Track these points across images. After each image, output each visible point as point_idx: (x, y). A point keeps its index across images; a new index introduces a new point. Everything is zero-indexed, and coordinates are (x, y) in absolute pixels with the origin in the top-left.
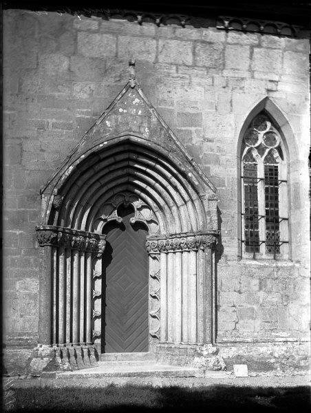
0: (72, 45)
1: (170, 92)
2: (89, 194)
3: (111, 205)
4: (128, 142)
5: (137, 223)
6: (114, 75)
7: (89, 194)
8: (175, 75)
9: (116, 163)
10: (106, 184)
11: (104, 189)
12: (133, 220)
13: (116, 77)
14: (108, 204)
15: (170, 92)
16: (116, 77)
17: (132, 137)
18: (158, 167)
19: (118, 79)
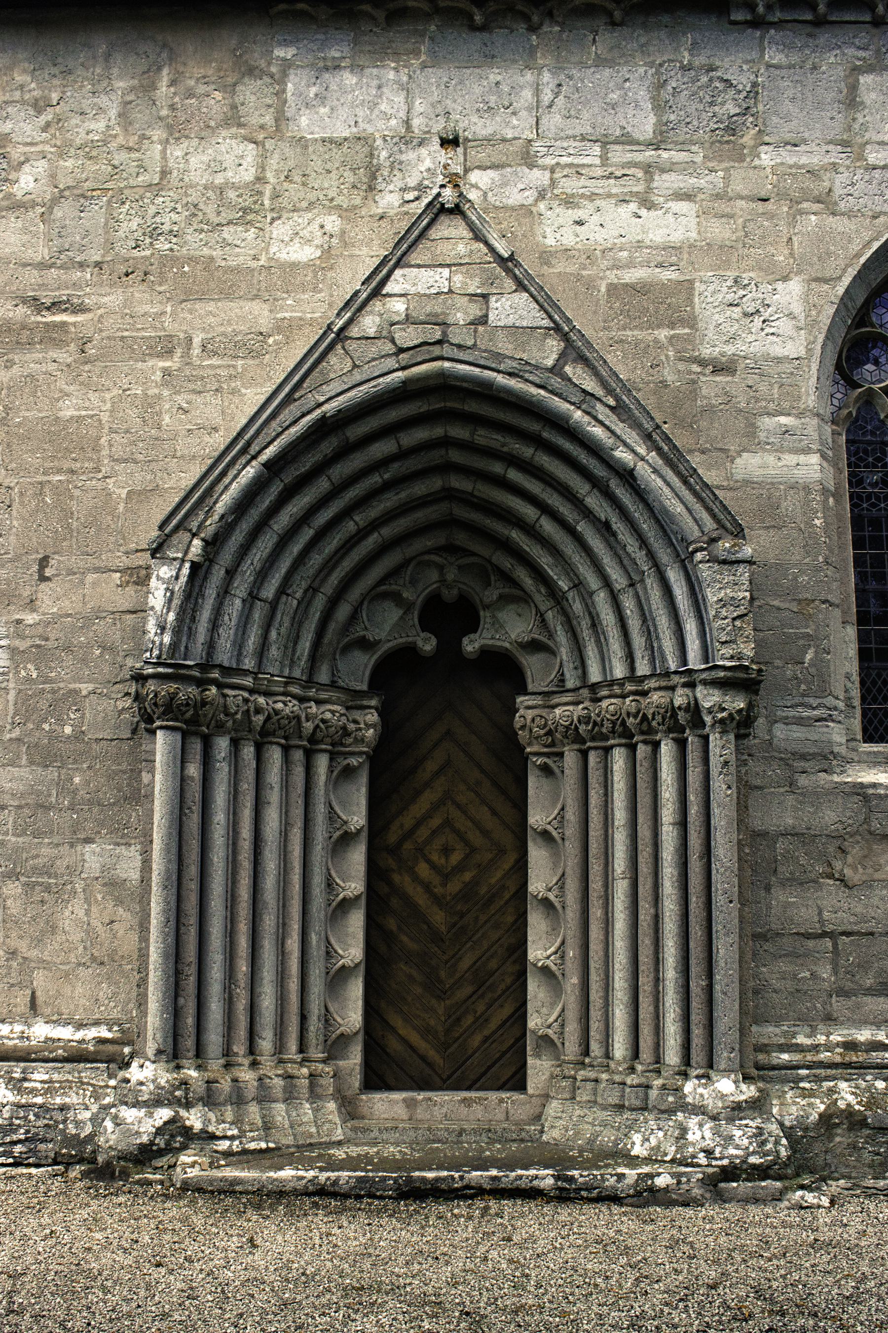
0: (269, 106)
1: (580, 223)
2: (316, 560)
3: (396, 598)
4: (443, 386)
5: (488, 655)
6: (400, 184)
7: (316, 560)
8: (599, 172)
9: (402, 455)
10: (374, 526)
11: (371, 542)
12: (471, 645)
13: (404, 190)
14: (385, 596)
15: (580, 223)
16: (404, 190)
17: (447, 364)
18: (545, 461)
19: (410, 196)
